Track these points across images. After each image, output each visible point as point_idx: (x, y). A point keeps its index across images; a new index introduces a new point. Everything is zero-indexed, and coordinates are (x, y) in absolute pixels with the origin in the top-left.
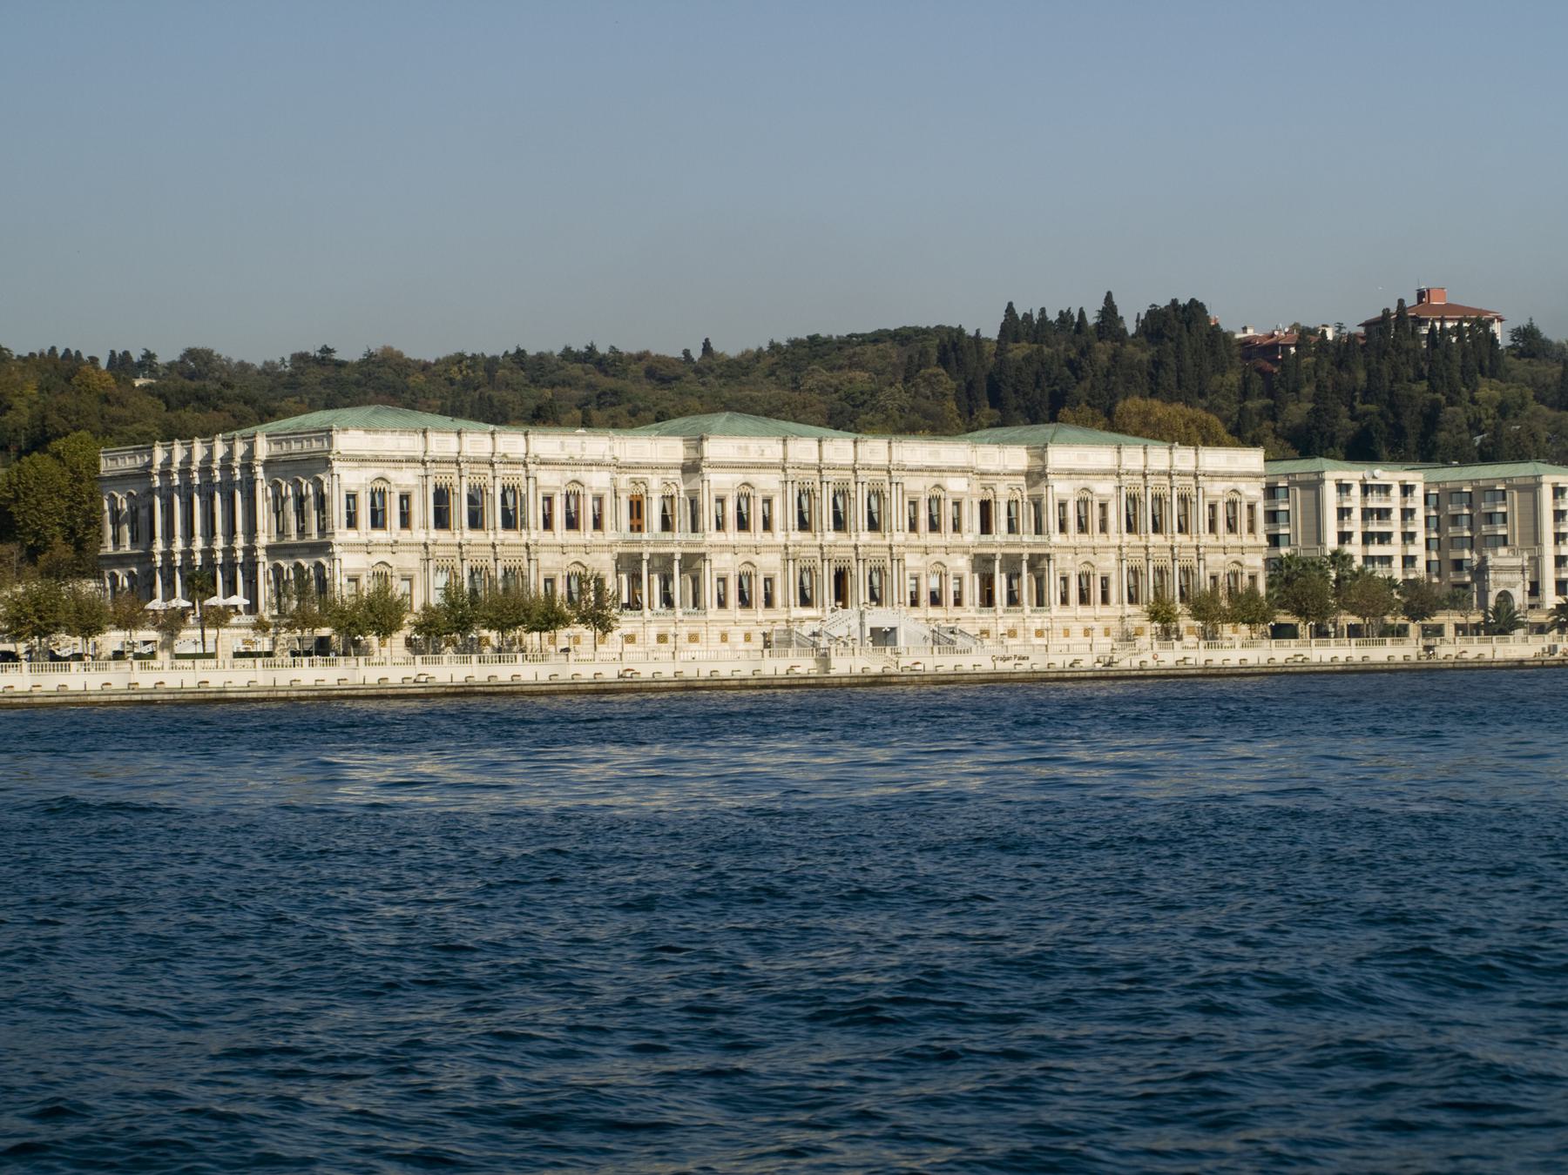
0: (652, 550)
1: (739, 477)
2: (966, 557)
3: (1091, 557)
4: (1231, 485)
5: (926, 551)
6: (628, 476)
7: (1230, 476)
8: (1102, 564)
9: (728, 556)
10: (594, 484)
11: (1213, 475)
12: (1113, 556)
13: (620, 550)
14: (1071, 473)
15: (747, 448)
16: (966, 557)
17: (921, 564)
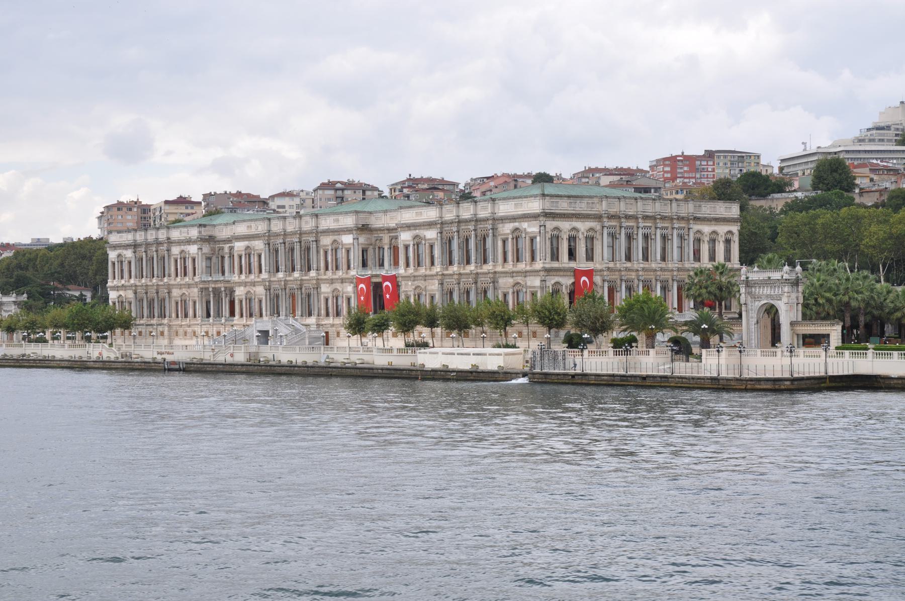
1: (246, 243)
3: (421, 283)
4: (516, 224)
7: (513, 219)
9: (242, 288)
14: (409, 227)
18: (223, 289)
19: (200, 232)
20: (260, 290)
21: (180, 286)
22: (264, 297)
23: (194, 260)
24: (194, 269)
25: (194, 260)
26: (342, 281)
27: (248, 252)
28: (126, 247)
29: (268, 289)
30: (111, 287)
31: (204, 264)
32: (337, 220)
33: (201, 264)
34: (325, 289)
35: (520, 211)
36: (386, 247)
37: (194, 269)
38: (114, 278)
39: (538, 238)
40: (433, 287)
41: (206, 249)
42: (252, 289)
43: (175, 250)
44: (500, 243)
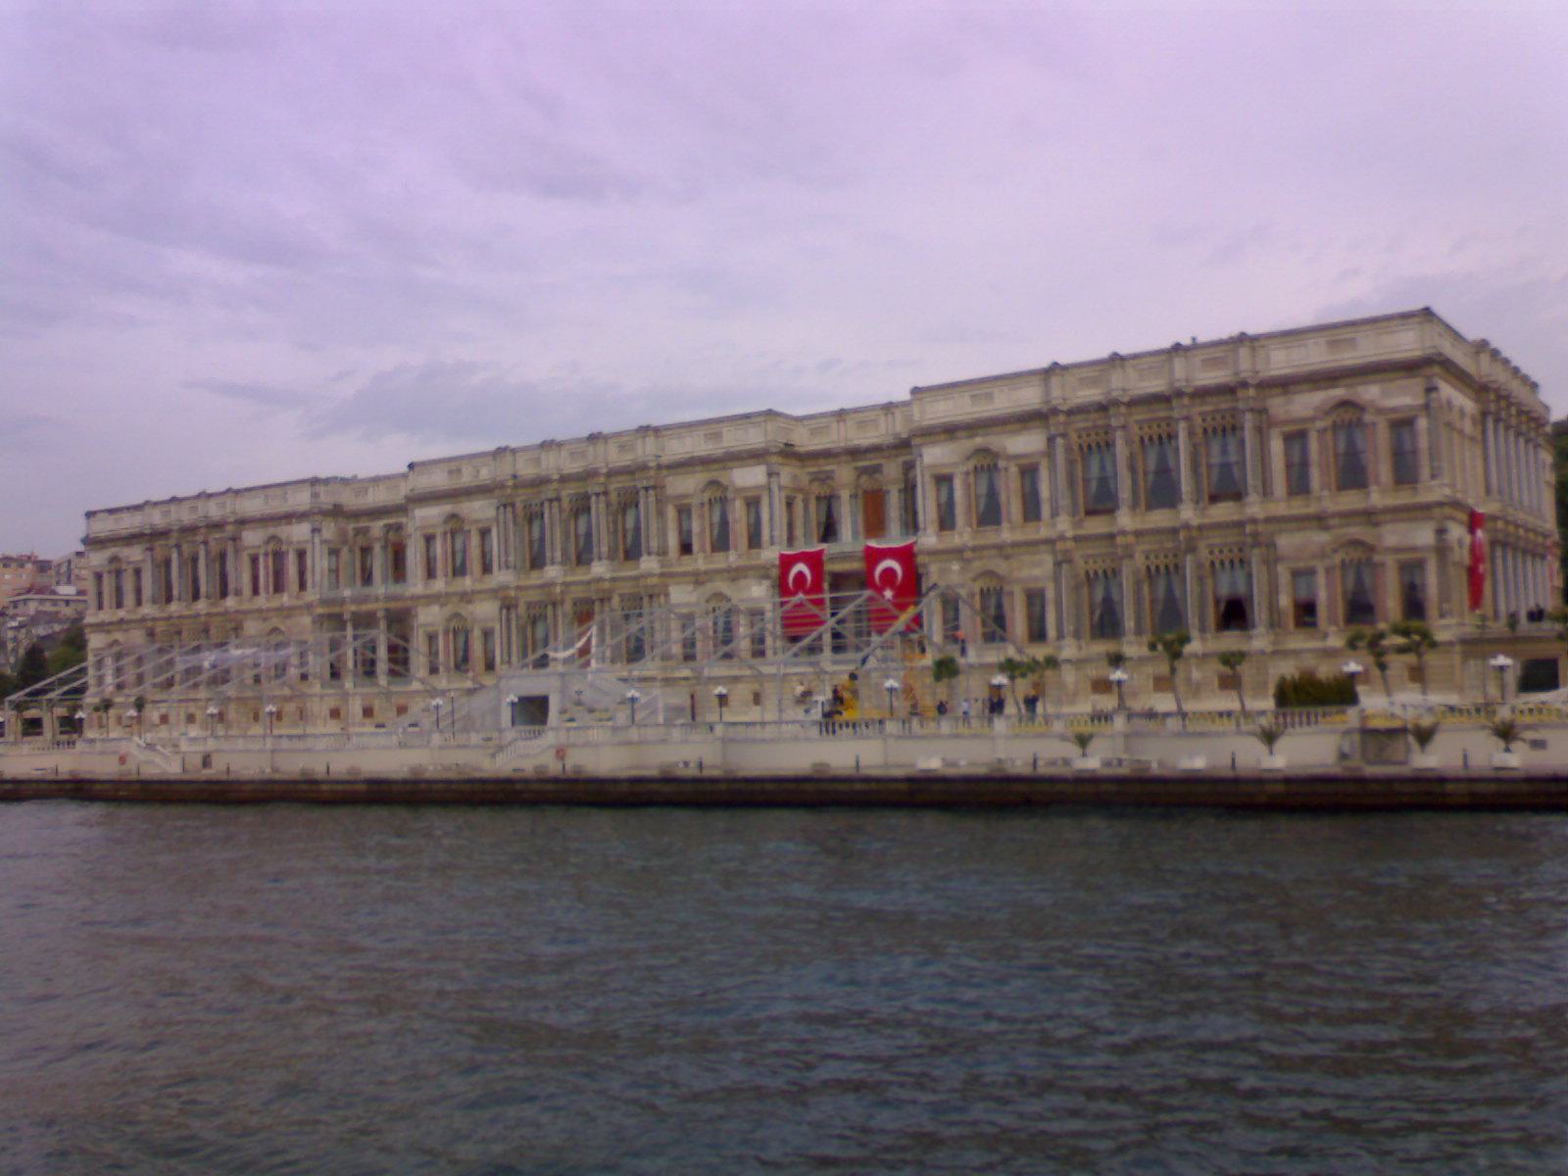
0: (353, 608)
1: (447, 508)
2: (766, 583)
4: (1339, 393)
5: (698, 579)
6: (381, 523)
8: (1025, 573)
9: (435, 609)
10: (295, 539)
11: (1286, 384)
12: (1048, 560)
13: (320, 611)
14: (950, 431)
15: (459, 471)
16: (766, 583)
17: (693, 599)
18: (380, 614)
19: (315, 495)
20: (485, 610)
21: (262, 614)
22: (497, 627)
23: (301, 555)
24: (302, 573)
25: (301, 555)
26: (736, 574)
27: (455, 525)
28: (131, 539)
29: (508, 606)
30: (91, 625)
31: (326, 563)
32: (718, 436)
33: (319, 563)
34: (681, 595)
35: (1349, 358)
36: (845, 494)
37: (302, 573)
38: (100, 607)
39: (1422, 423)
40: (1037, 572)
41: (329, 530)
42: (466, 610)
43: (252, 538)
44: (1276, 446)
